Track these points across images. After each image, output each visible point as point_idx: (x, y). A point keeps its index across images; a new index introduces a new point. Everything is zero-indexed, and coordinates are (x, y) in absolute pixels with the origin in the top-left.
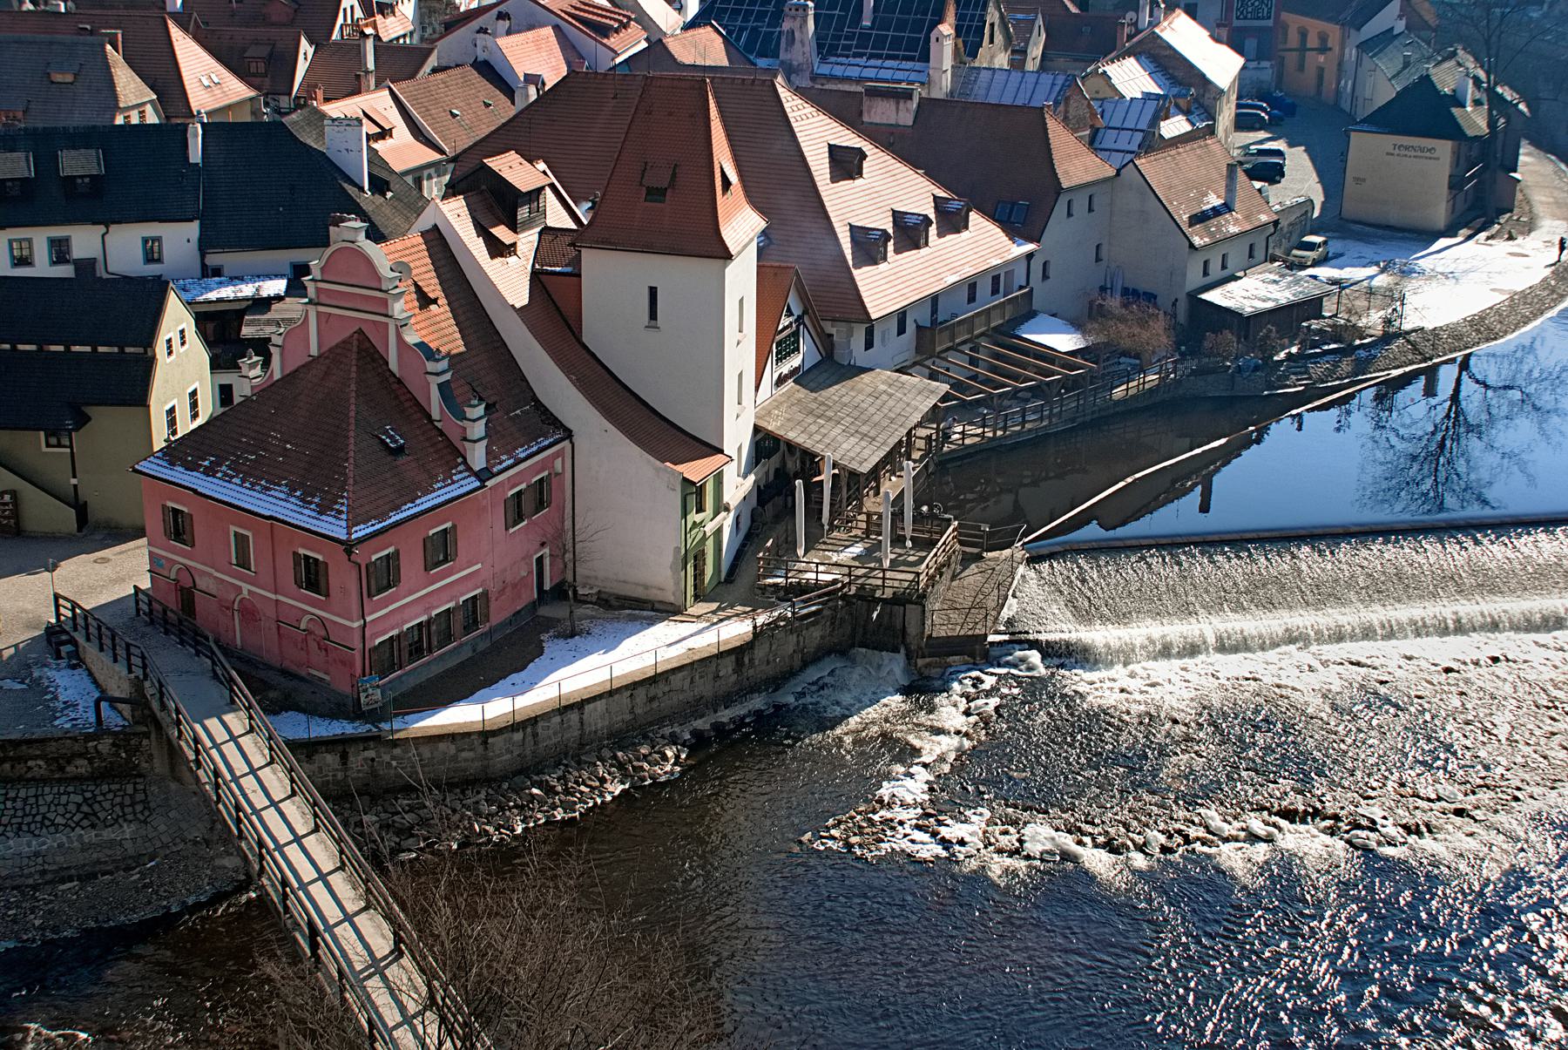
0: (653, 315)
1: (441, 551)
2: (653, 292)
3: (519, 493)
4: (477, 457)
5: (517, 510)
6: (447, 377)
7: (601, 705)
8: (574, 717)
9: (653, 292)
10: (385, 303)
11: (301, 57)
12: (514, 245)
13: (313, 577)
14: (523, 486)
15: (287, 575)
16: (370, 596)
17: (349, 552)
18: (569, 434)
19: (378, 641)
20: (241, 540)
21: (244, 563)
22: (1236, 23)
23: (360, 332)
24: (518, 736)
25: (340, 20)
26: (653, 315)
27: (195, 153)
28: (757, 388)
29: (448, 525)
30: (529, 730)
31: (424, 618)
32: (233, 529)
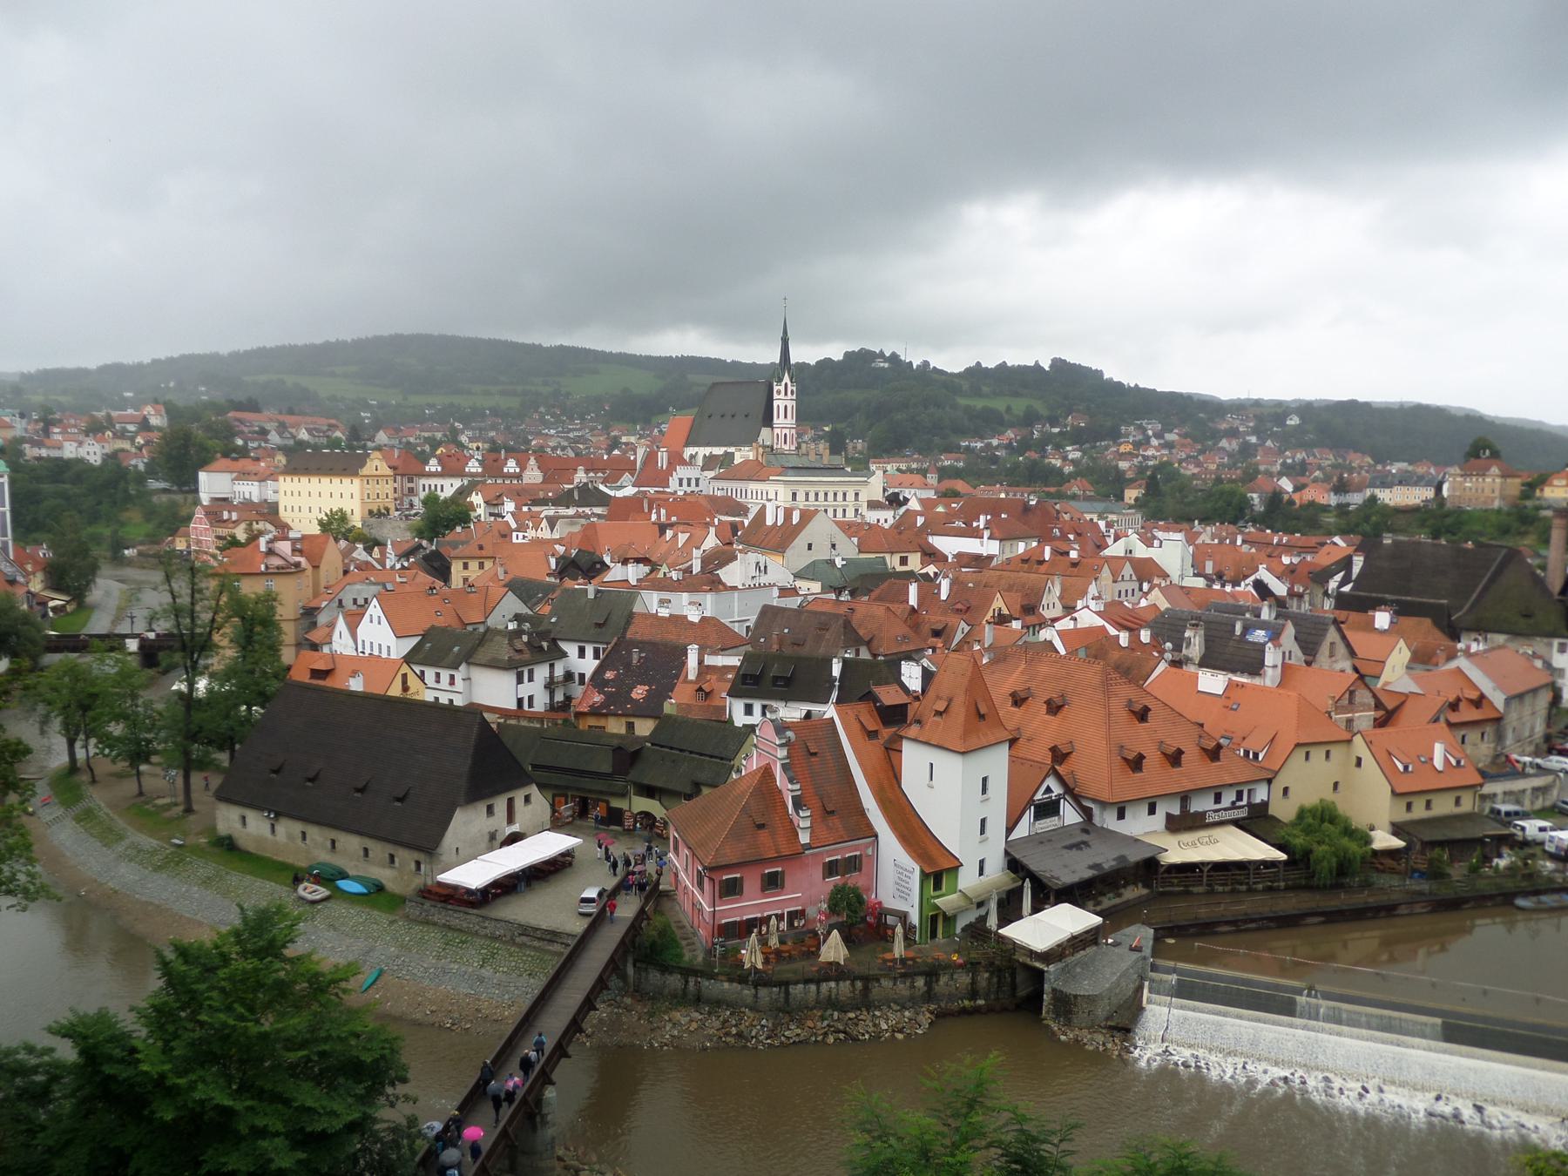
1: (773, 882)
4: (804, 838)
5: (831, 869)
6: (799, 793)
9: (932, 764)
11: (960, 629)
12: (876, 732)
14: (839, 857)
18: (876, 836)
21: (686, 870)
23: (769, 764)
25: (990, 613)
27: (836, 669)
28: (1009, 830)
30: (783, 988)
31: (759, 915)
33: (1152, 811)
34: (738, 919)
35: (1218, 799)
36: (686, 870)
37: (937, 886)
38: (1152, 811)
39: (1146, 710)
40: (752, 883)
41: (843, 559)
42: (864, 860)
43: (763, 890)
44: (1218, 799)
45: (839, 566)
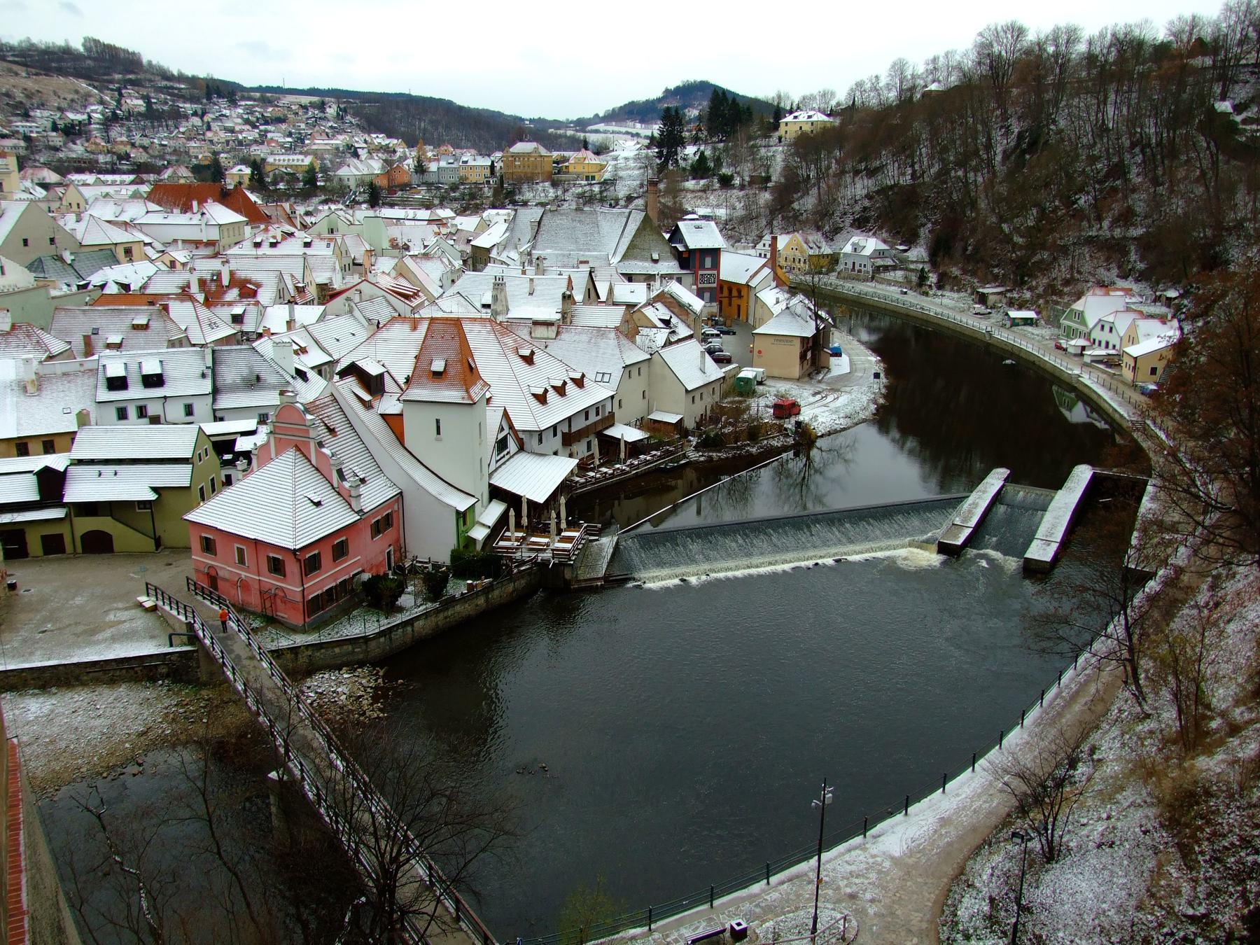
0: (438, 433)
2: (438, 421)
3: (378, 521)
7: (421, 623)
8: (409, 629)
9: (438, 421)
10: (307, 431)
13: (277, 567)
14: (379, 517)
15: (264, 566)
16: (306, 575)
17: (295, 555)
19: (310, 597)
20: (241, 551)
21: (242, 561)
22: (700, 286)
24: (382, 640)
26: (438, 433)
29: (344, 538)
31: (334, 584)
32: (236, 545)
33: (555, 435)
34: (319, 592)
35: (587, 418)
36: (242, 561)
37: (465, 524)
38: (555, 435)
39: (533, 353)
40: (326, 559)
41: (71, 254)
42: (394, 515)
43: (334, 561)
44: (587, 418)
45: (69, 262)
